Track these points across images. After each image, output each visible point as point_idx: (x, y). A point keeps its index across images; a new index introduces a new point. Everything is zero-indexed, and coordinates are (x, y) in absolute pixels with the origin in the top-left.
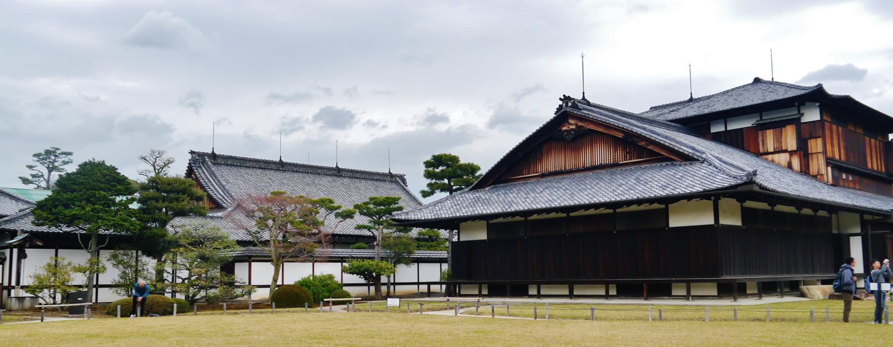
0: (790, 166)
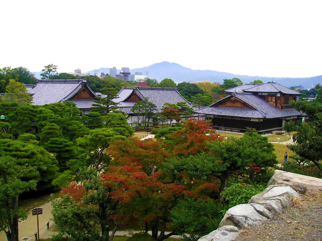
0: (273, 105)
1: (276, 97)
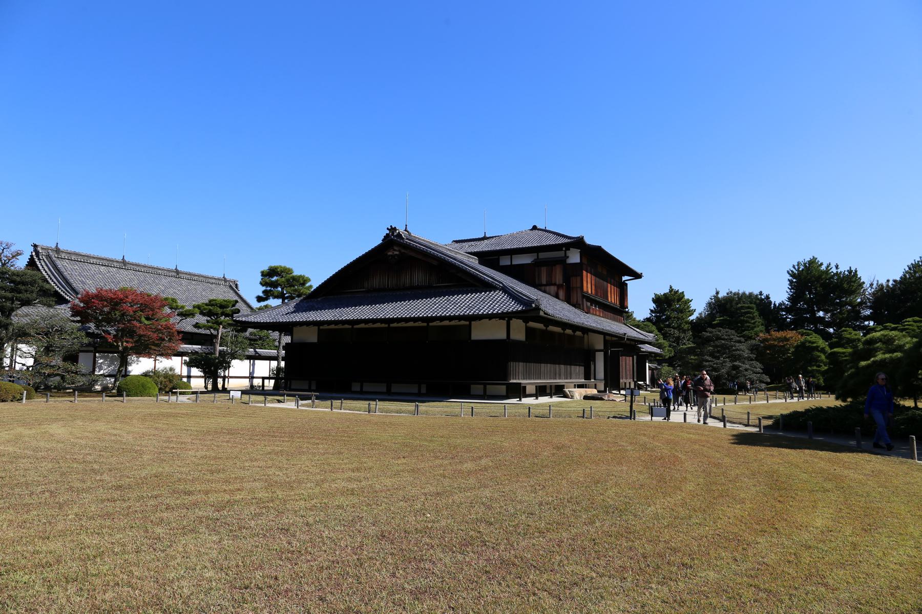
1: (562, 261)
